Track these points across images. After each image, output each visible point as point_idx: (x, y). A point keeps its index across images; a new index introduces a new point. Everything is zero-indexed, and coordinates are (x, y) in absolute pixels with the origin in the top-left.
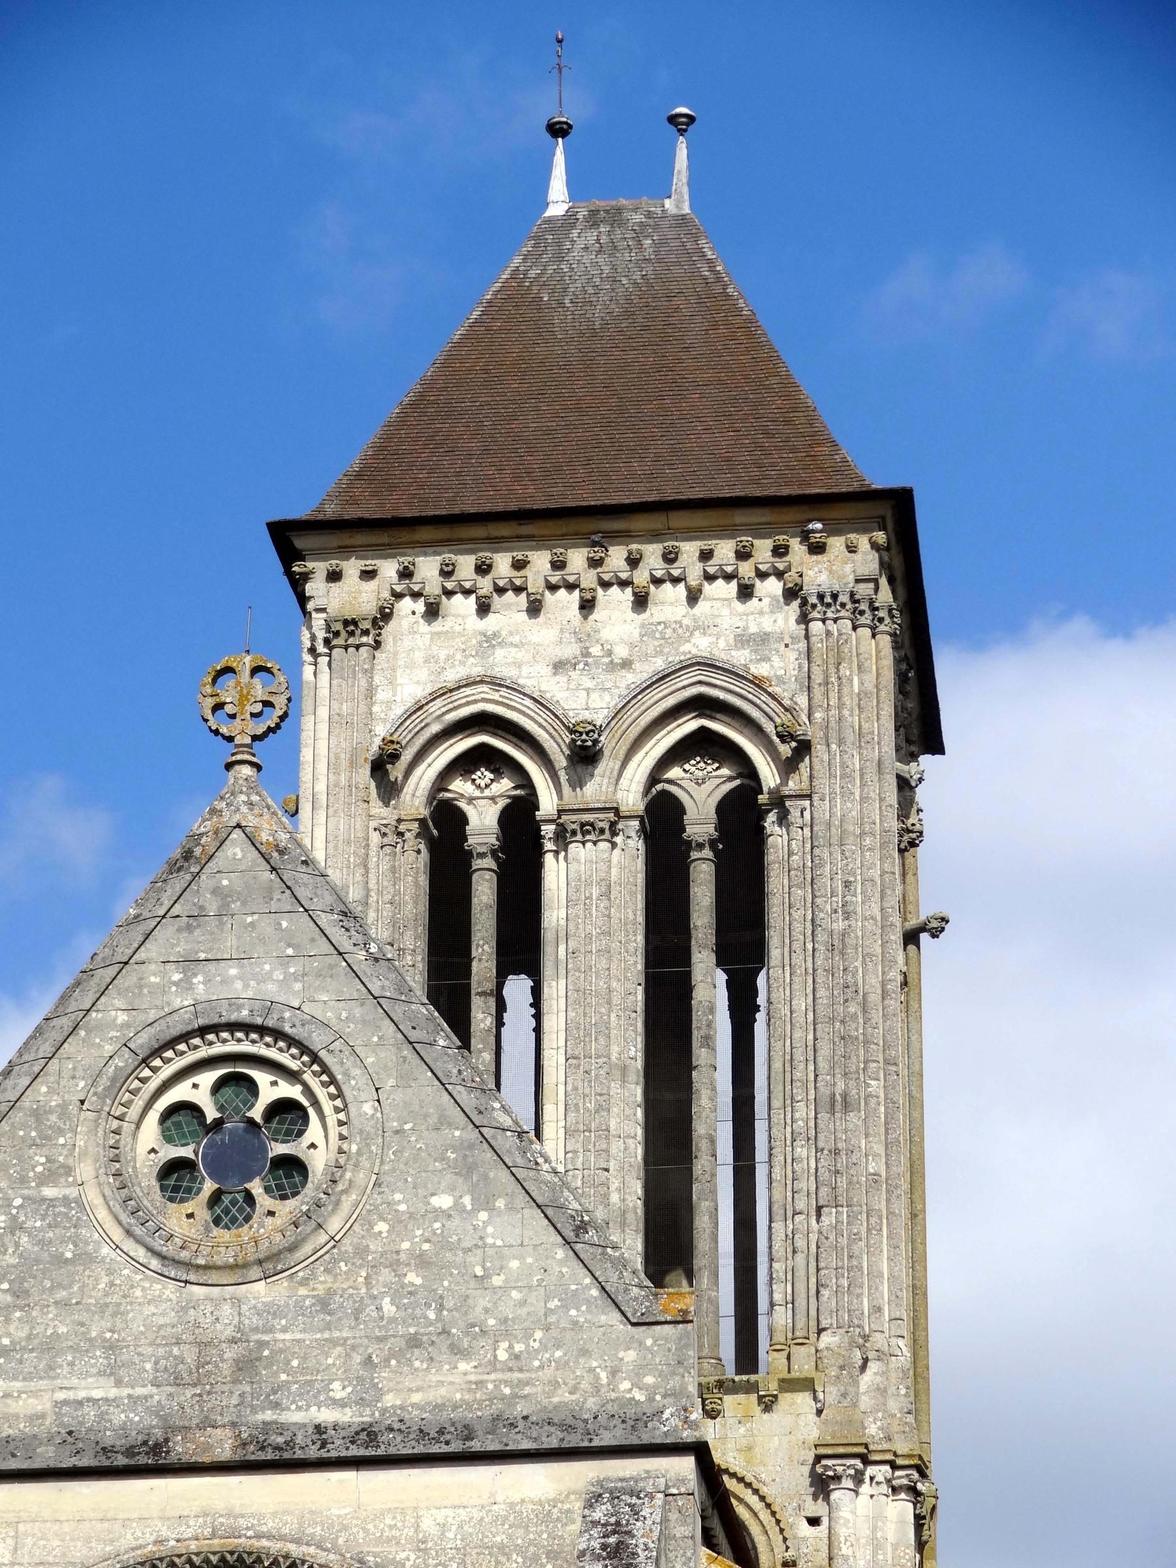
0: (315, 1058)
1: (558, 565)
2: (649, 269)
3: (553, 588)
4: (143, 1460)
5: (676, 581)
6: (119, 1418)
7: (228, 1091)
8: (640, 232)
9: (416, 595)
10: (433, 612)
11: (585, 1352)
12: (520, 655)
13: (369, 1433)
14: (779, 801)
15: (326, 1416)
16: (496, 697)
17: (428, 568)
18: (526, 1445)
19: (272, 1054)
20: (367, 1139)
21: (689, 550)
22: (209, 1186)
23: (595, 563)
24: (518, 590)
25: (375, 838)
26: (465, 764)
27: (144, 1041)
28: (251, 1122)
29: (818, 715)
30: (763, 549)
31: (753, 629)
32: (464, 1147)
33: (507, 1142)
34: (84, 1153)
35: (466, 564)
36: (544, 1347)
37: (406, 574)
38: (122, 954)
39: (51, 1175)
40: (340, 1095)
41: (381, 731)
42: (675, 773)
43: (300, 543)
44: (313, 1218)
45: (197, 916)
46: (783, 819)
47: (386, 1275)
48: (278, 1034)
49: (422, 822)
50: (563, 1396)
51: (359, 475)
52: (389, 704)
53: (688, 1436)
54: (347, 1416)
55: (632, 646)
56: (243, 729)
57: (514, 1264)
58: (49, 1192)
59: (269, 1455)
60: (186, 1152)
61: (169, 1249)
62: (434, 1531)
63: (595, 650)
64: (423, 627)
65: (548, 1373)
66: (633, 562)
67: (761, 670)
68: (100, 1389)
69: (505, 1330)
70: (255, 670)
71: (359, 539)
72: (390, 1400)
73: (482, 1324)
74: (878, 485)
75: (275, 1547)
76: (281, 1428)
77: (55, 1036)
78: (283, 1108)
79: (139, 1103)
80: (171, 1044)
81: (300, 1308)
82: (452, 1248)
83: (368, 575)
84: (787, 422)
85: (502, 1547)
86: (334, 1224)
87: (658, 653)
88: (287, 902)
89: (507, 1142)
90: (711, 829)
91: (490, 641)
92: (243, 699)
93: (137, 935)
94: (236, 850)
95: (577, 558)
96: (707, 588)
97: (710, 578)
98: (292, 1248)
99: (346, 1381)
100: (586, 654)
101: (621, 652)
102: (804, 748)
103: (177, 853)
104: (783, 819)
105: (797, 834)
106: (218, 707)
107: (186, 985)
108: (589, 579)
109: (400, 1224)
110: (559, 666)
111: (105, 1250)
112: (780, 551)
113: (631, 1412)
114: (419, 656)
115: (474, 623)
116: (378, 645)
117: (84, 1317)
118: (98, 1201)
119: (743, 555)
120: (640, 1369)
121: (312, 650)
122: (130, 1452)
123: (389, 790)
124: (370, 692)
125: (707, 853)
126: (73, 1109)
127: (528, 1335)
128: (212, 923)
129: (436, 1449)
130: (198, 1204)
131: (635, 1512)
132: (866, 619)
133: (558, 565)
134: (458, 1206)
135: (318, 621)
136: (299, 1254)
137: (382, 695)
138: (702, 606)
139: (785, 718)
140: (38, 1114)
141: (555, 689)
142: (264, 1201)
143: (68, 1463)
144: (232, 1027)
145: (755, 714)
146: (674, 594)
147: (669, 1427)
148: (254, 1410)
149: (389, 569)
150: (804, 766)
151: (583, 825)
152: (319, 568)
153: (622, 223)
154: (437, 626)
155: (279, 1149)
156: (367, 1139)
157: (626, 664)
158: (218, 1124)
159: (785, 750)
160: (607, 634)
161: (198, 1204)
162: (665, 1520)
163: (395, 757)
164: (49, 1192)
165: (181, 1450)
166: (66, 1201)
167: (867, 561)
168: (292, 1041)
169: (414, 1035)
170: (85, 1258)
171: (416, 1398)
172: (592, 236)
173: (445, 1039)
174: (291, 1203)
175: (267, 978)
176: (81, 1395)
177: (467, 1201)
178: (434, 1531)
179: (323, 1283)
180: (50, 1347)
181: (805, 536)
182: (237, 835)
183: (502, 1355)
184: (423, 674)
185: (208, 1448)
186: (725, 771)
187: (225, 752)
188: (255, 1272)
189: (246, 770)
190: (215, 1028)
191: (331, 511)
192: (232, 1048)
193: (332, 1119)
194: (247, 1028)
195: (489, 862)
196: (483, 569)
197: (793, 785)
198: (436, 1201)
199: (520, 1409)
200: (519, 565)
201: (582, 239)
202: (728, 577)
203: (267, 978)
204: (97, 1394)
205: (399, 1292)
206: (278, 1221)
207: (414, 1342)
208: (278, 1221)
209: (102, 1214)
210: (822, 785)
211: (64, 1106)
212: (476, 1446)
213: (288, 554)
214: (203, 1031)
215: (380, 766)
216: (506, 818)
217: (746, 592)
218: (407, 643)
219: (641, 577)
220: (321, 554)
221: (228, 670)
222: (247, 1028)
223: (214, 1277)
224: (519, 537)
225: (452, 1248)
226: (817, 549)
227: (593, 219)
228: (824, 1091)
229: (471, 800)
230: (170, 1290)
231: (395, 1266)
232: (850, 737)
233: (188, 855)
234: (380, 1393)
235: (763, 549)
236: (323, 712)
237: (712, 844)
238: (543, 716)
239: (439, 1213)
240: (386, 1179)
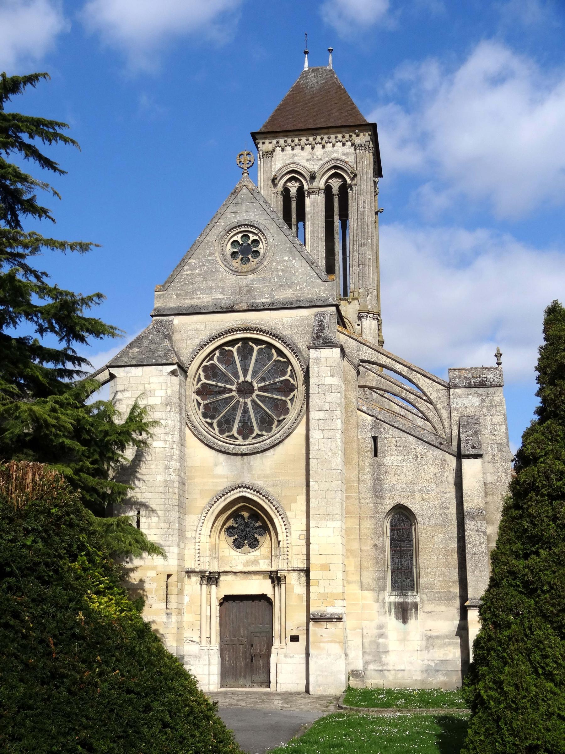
0: (261, 231)
1: (307, 140)
2: (324, 81)
3: (306, 145)
4: (229, 310)
5: (330, 143)
6: (224, 302)
7: (244, 238)
8: (322, 74)
9: (280, 147)
10: (283, 150)
11: (314, 287)
12: (300, 158)
13: (273, 304)
14: (351, 186)
15: (264, 300)
17: (282, 141)
18: (303, 305)
19: (252, 230)
20: (271, 246)
21: (333, 136)
22: (241, 256)
23: (314, 139)
24: (300, 145)
25: (273, 195)
26: (290, 180)
27: (227, 228)
28: (248, 244)
29: (358, 169)
30: (347, 136)
31: (345, 152)
32: (289, 248)
33: (298, 247)
34: (216, 251)
35: (289, 140)
36: (306, 286)
37: (278, 142)
38: (223, 211)
39: (211, 254)
40: (266, 238)
41: (273, 174)
42: (330, 181)
43: (257, 137)
44: (261, 262)
45: (237, 204)
46: (351, 190)
47: (275, 273)
48: (253, 226)
49: (282, 191)
50: (310, 296)
51: (268, 123)
52: (275, 168)
53: (334, 303)
54: (268, 300)
56: (245, 166)
57: (300, 270)
58: (210, 258)
59: (254, 308)
60: (236, 250)
61: (233, 269)
62: (285, 322)
63: (315, 157)
64: (281, 153)
65: (307, 291)
66: (322, 139)
67: (347, 160)
68: (220, 296)
69: (299, 283)
70: (247, 154)
71: (268, 136)
72: (276, 297)
73: (294, 282)
74: (370, 122)
75: (255, 326)
76: (256, 303)
77: (210, 228)
78: (255, 242)
79: (227, 240)
80: (233, 229)
81: (259, 279)
82: (288, 267)
83: (270, 143)
84: (352, 110)
85: (298, 325)
86: (265, 263)
87: (327, 157)
88: (255, 200)
89: (298, 247)
90: (338, 192)
91: (294, 155)
92: (245, 160)
93: (225, 208)
94: (244, 190)
95: (311, 139)
96: (336, 144)
97: (337, 142)
98: (257, 268)
99: (268, 294)
100: (313, 158)
101: (320, 157)
102: (355, 175)
103: (233, 191)
104: (351, 190)
105: (354, 192)
106: (240, 162)
107: (235, 217)
108: (313, 143)
109: (278, 263)
110: (308, 160)
111: (221, 269)
112: (350, 136)
113: (323, 299)
114: (280, 159)
115: (291, 151)
116: (272, 157)
117: (217, 282)
118: (219, 260)
119: (343, 137)
120: (325, 290)
121: (260, 158)
122: (227, 308)
123: (275, 185)
124: (271, 166)
125: (337, 196)
126: (214, 242)
127: (303, 284)
128: (240, 205)
129: (285, 306)
130: (238, 260)
131: (324, 318)
132: (367, 150)
133: (307, 140)
134: (289, 259)
135: (261, 152)
136: (258, 269)
137: (273, 167)
138: (335, 148)
139: (352, 169)
140: (207, 243)
141: (307, 165)
142: (251, 259)
143: (215, 310)
144: (244, 225)
145: (346, 169)
147: (331, 301)
148: (250, 300)
149: (274, 142)
150: (355, 179)
152: (261, 142)
153: (319, 72)
154: (284, 153)
155: (254, 249)
156: (271, 246)
157: (321, 159)
158: (242, 244)
159: (352, 176)
160: (317, 153)
161: (238, 260)
162: (330, 319)
163: (276, 179)
164: (210, 258)
165: (236, 307)
166: (213, 260)
167: (367, 138)
168: (256, 228)
169: (280, 226)
170: (217, 271)
171: (281, 297)
172: (313, 74)
173: (286, 227)
174: (257, 260)
175: (250, 216)
176: (217, 297)
177: (291, 258)
178: (285, 322)
179: (263, 275)
180: (211, 288)
181: (355, 133)
182: (244, 187)
183: (298, 288)
184: (281, 162)
185: (242, 307)
186: (340, 180)
187: (242, 171)
188: (250, 273)
189: (246, 174)
190: (241, 225)
191: (263, 130)
192: (244, 229)
193: (264, 243)
194: (247, 225)
195: (295, 199)
196: (293, 141)
197: (353, 183)
198: (285, 258)
199: (302, 298)
200: (300, 140)
201: (311, 75)
202: (340, 142)
203: (250, 216)
204: (220, 297)
205: (278, 276)
206: (254, 263)
207: (281, 286)
208: (254, 263)
209: (220, 262)
210: (359, 182)
211: (212, 241)
212: (293, 306)
213: (255, 139)
214: (239, 226)
215: (273, 180)
217: (344, 145)
218: (278, 156)
219: (323, 142)
220: (261, 139)
221: (242, 154)
222: (247, 225)
223: (242, 274)
224: (300, 135)
225: (288, 267)
226: (358, 136)
227: (313, 71)
228: (360, 242)
230: (234, 277)
231: (277, 271)
232: (364, 173)
233: (235, 191)
234: (275, 296)
235: (347, 136)
236: (262, 170)
237: (338, 195)
238: (305, 170)
239: (285, 261)
240: (275, 254)
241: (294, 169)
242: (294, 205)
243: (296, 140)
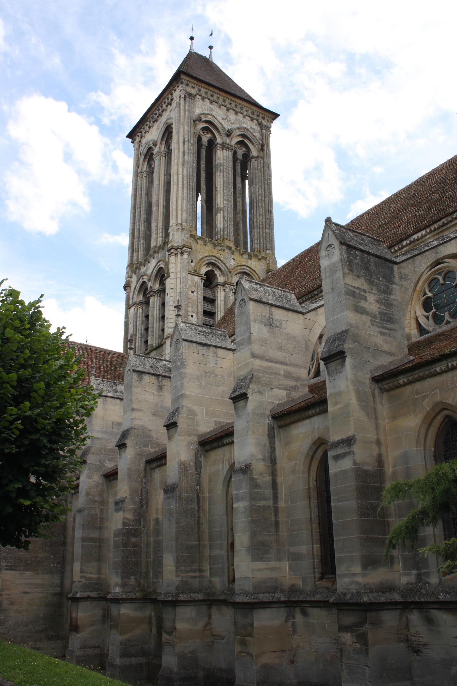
16: (213, 119)
24: (217, 103)
26: (204, 129)
55: (234, 121)
63: (228, 119)
101: (232, 121)
110: (223, 119)
146: (240, 114)
151: (228, 147)
195: (205, 148)
196: (212, 96)
216: (208, 141)
229: (203, 136)
238: (220, 126)
241: (212, 120)
242: (203, 152)
243: (216, 96)
